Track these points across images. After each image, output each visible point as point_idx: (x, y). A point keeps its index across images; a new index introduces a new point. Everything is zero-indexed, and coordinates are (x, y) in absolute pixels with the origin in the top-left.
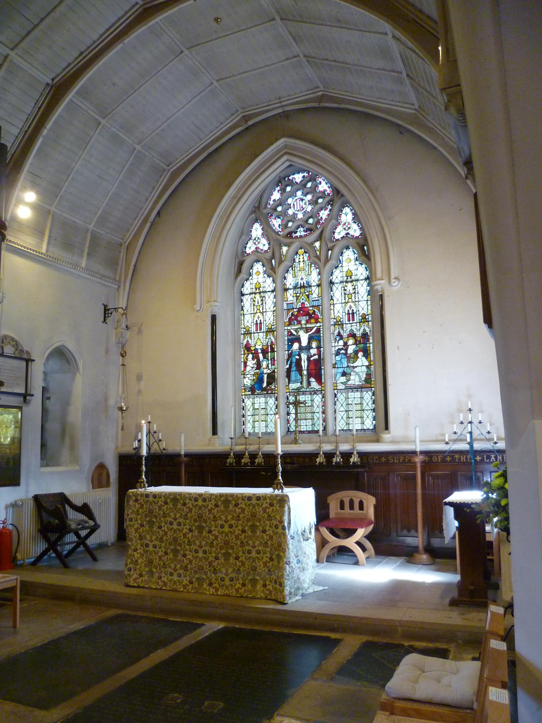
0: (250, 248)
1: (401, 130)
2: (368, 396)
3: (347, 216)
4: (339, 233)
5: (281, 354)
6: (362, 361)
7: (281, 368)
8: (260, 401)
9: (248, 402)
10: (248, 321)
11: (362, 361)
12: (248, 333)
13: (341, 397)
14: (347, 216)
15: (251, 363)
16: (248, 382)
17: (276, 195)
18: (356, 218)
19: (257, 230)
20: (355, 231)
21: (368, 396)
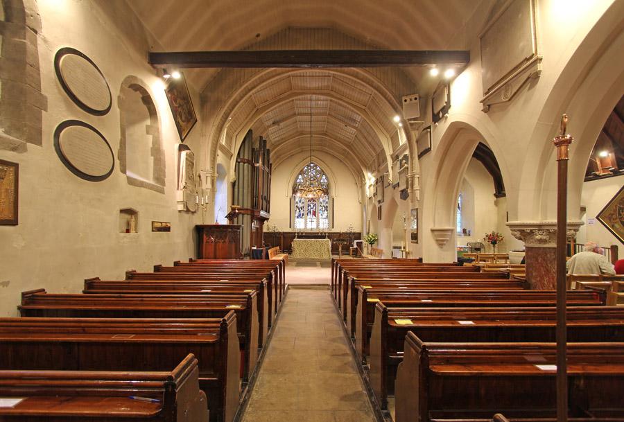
0: (298, 181)
1: (341, 161)
2: (327, 220)
3: (324, 177)
4: (322, 181)
5: (306, 209)
6: (326, 212)
7: (305, 214)
8: (300, 220)
9: (297, 220)
10: (297, 200)
11: (326, 212)
12: (297, 203)
13: (320, 221)
14: (324, 177)
15: (298, 211)
16: (297, 215)
17: (306, 168)
18: (327, 178)
19: (300, 177)
20: (326, 181)
21: (327, 220)
